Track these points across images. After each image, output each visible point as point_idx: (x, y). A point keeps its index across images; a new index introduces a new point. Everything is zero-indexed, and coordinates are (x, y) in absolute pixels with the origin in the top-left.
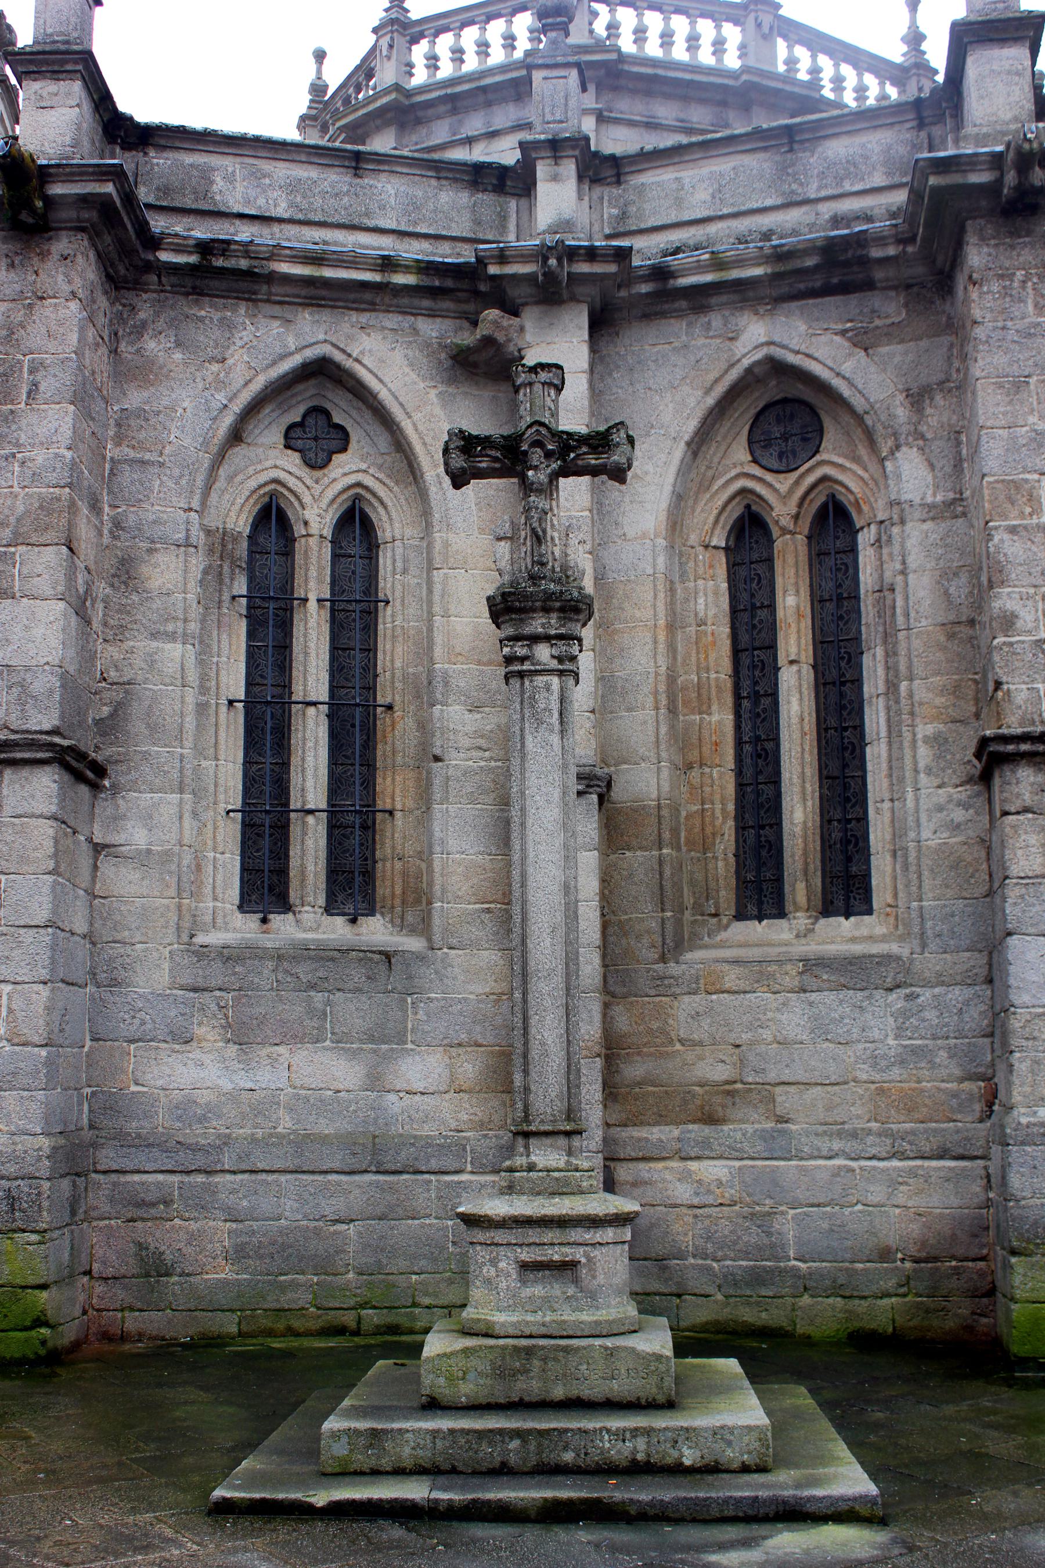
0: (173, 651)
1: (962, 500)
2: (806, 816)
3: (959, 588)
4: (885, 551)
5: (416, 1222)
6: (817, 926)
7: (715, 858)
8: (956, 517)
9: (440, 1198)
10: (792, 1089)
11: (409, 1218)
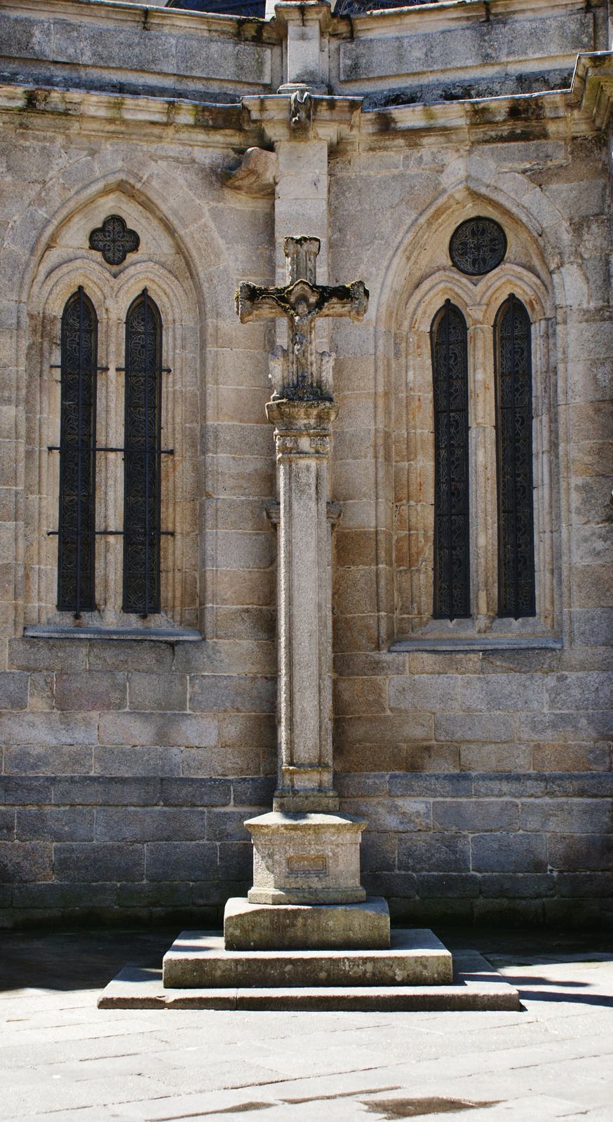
1: (609, 307)
2: (487, 542)
4: (551, 341)
5: (193, 843)
7: (418, 571)
8: (604, 320)
9: (210, 825)
11: (187, 840)
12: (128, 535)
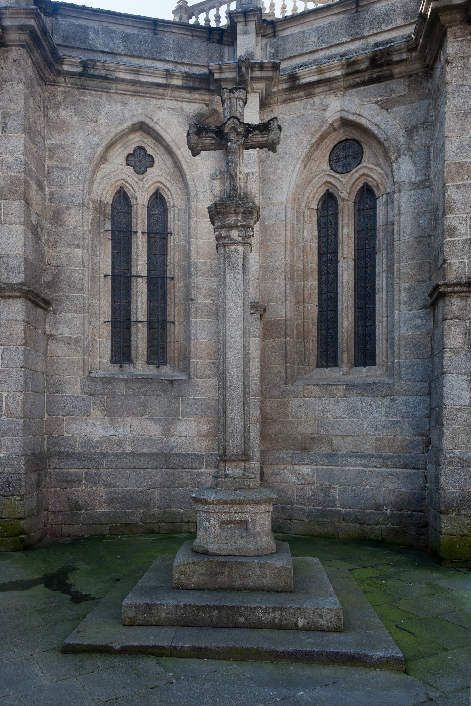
0: (79, 253)
2: (348, 324)
3: (425, 221)
4: (390, 207)
6: (351, 370)
7: (308, 342)
10: (339, 438)
12: (150, 324)
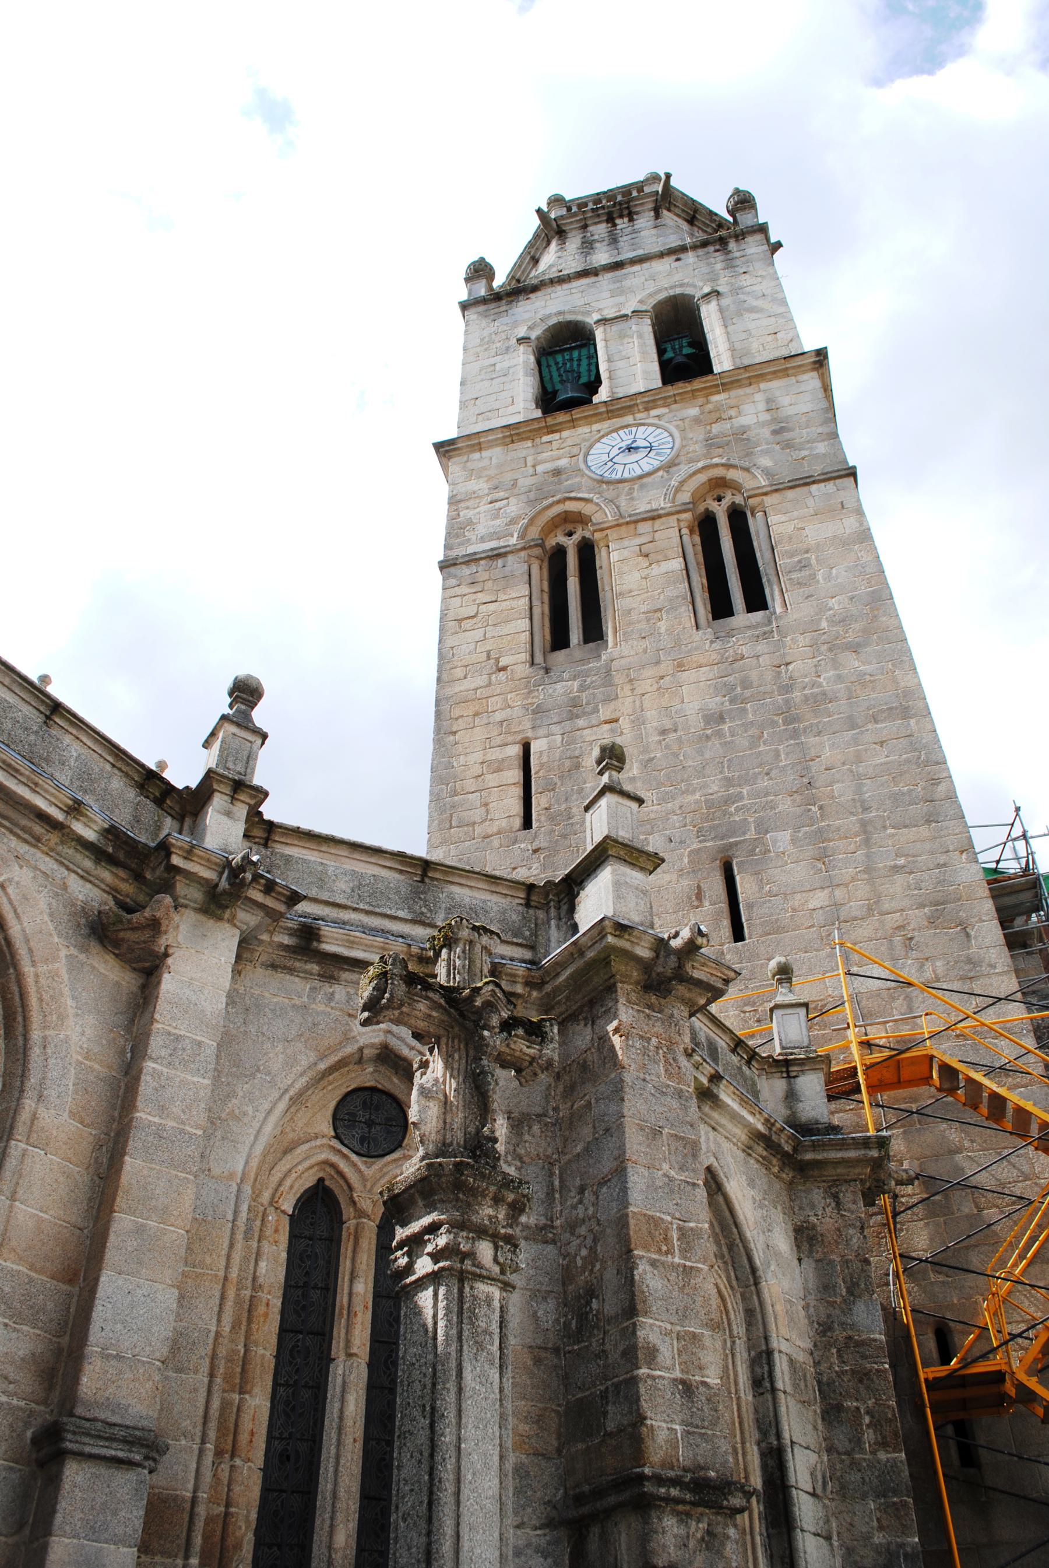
1: (553, 1227)
8: (546, 1242)
